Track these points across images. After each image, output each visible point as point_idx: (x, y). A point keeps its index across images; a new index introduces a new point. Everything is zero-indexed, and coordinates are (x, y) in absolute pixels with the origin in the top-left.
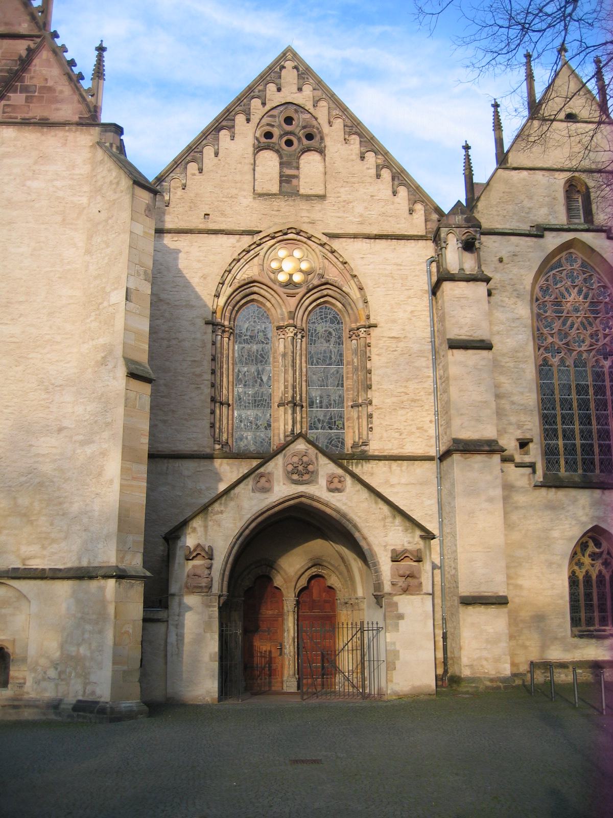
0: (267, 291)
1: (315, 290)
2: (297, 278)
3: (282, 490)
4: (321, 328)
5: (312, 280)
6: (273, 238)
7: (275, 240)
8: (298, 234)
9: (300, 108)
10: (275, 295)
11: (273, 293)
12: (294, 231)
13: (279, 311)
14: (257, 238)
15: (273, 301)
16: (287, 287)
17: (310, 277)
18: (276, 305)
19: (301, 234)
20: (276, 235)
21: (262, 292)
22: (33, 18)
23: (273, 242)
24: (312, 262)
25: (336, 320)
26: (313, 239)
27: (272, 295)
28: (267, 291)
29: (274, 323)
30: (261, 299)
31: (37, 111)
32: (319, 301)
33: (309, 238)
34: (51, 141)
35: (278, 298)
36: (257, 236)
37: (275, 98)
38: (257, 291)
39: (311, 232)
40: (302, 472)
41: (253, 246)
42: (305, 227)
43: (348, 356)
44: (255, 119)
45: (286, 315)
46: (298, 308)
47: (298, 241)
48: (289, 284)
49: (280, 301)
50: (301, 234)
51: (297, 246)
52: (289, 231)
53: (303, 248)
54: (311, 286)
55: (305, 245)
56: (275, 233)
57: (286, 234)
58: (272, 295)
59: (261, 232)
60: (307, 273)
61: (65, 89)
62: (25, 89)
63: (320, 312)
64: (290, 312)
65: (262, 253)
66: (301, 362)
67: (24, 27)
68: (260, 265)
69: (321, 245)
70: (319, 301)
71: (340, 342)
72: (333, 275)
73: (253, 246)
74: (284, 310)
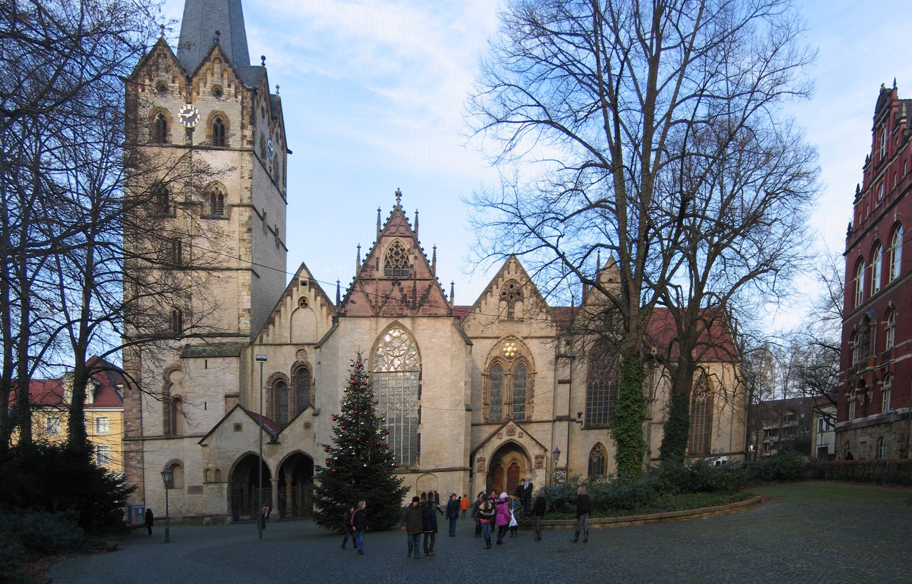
2: (512, 354)
3: (505, 438)
4: (519, 374)
9: (516, 282)
22: (430, 271)
25: (524, 370)
31: (434, 311)
34: (438, 323)
37: (507, 277)
40: (511, 432)
43: (527, 384)
44: (500, 286)
48: (510, 357)
61: (441, 301)
62: (429, 302)
66: (512, 388)
67: (427, 275)
71: (525, 378)
72: (524, 353)
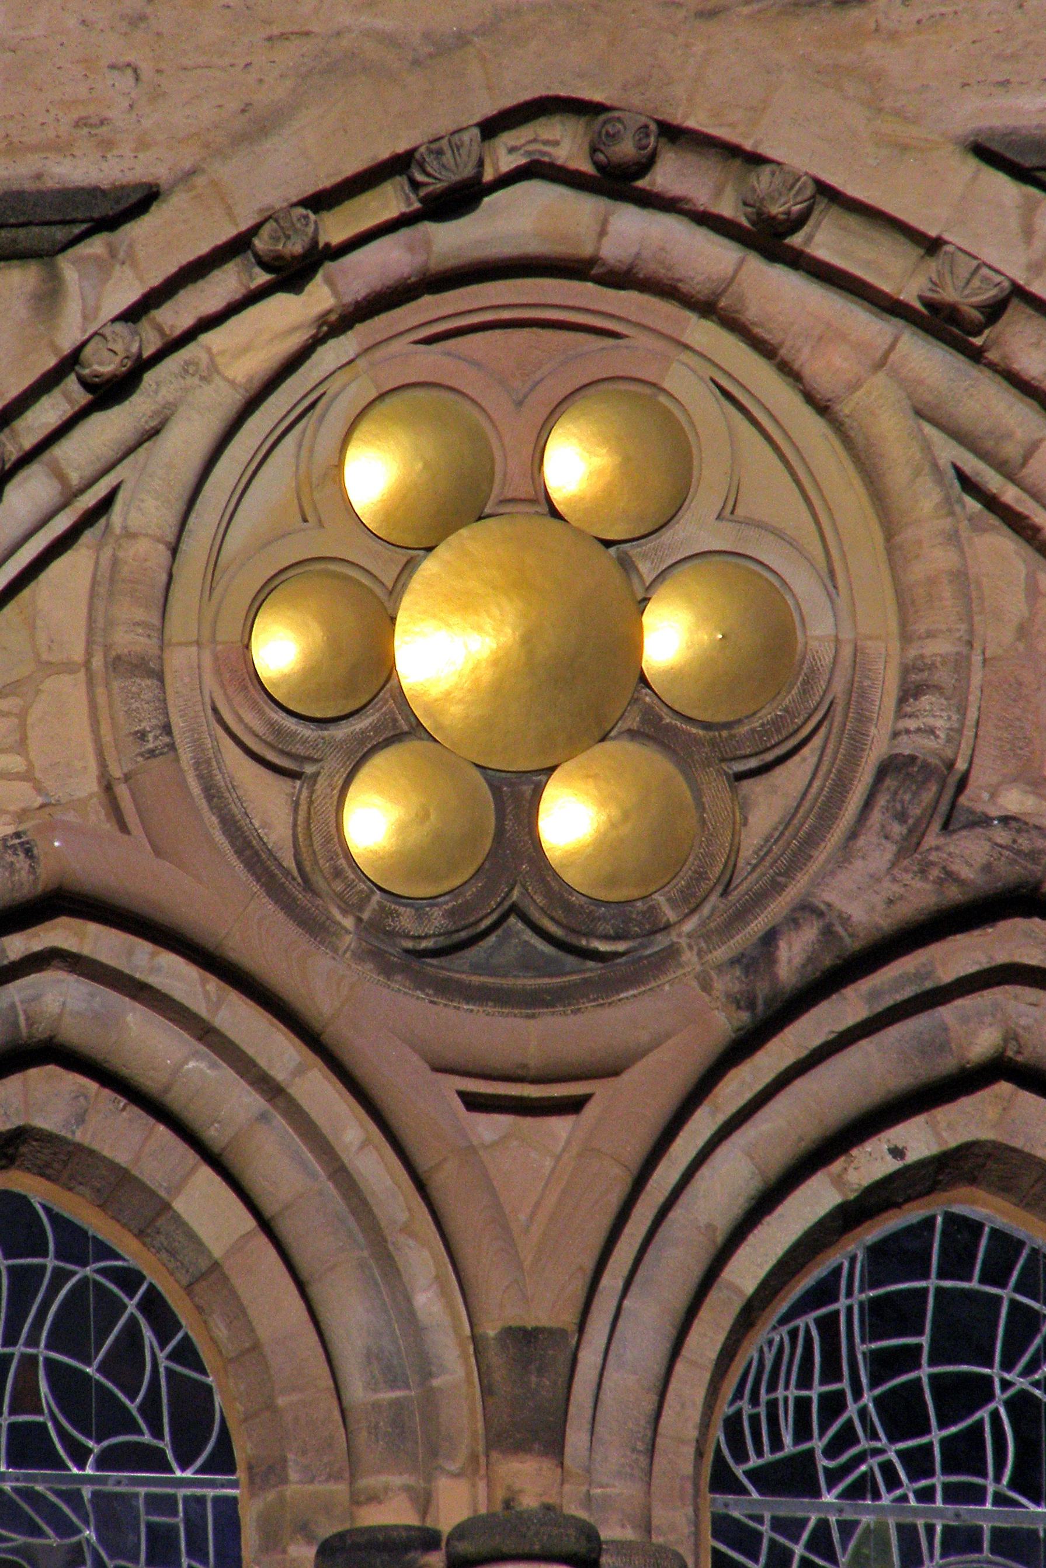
0: (205, 1033)
1: (849, 1007)
5: (796, 845)
6: (291, 274)
7: (318, 297)
8: (617, 181)
10: (319, 1092)
11: (279, 1051)
12: (565, 142)
13: (354, 1316)
14: (98, 288)
15: (279, 1166)
16: (458, 968)
17: (770, 802)
18: (317, 1238)
19: (669, 175)
20: (336, 227)
21: (147, 1043)
23: (288, 315)
24: (804, 585)
26: (827, 240)
27: (271, 1089)
28: (205, 1033)
29: (269, 1473)
30: (118, 1134)
32: (871, 1163)
33: (769, 237)
35: (350, 1129)
36: (104, 267)
38: (75, 1033)
39: (801, 142)
41: (47, 414)
42: (718, 77)
45: (454, 1368)
46: (612, 1281)
47: (622, 278)
48: (494, 916)
49: (376, 1169)
50: (669, 175)
51: (597, 357)
52: (504, 156)
53: (685, 384)
54: (794, 956)
55: (703, 333)
56: (321, 201)
57: (458, 200)
58: (271, 1089)
59: (144, 199)
60: (704, 744)
63: (887, 1315)
64: (525, 1340)
65: (145, 508)
68: (118, 664)
69: (945, 324)
70: (871, 1163)
73: (47, 414)
74: (427, 1301)
